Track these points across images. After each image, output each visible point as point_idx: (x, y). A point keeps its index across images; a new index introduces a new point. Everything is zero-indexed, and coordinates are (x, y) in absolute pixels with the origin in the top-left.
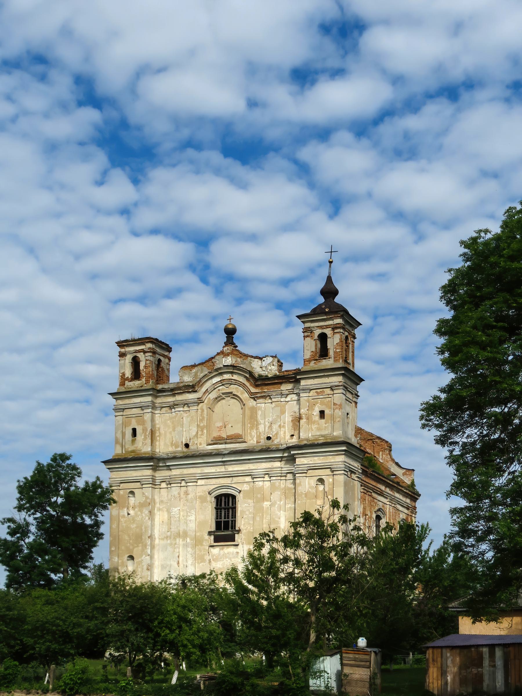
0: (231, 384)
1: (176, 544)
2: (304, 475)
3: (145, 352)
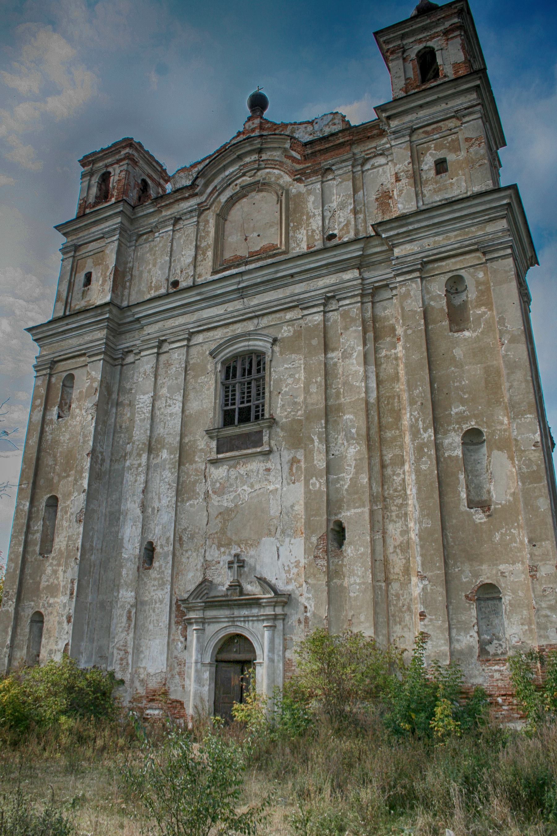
0: (258, 169)
1: (140, 465)
2: (417, 274)
3: (118, 162)
